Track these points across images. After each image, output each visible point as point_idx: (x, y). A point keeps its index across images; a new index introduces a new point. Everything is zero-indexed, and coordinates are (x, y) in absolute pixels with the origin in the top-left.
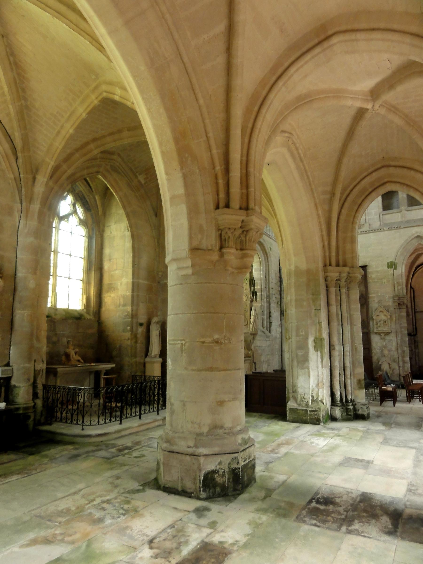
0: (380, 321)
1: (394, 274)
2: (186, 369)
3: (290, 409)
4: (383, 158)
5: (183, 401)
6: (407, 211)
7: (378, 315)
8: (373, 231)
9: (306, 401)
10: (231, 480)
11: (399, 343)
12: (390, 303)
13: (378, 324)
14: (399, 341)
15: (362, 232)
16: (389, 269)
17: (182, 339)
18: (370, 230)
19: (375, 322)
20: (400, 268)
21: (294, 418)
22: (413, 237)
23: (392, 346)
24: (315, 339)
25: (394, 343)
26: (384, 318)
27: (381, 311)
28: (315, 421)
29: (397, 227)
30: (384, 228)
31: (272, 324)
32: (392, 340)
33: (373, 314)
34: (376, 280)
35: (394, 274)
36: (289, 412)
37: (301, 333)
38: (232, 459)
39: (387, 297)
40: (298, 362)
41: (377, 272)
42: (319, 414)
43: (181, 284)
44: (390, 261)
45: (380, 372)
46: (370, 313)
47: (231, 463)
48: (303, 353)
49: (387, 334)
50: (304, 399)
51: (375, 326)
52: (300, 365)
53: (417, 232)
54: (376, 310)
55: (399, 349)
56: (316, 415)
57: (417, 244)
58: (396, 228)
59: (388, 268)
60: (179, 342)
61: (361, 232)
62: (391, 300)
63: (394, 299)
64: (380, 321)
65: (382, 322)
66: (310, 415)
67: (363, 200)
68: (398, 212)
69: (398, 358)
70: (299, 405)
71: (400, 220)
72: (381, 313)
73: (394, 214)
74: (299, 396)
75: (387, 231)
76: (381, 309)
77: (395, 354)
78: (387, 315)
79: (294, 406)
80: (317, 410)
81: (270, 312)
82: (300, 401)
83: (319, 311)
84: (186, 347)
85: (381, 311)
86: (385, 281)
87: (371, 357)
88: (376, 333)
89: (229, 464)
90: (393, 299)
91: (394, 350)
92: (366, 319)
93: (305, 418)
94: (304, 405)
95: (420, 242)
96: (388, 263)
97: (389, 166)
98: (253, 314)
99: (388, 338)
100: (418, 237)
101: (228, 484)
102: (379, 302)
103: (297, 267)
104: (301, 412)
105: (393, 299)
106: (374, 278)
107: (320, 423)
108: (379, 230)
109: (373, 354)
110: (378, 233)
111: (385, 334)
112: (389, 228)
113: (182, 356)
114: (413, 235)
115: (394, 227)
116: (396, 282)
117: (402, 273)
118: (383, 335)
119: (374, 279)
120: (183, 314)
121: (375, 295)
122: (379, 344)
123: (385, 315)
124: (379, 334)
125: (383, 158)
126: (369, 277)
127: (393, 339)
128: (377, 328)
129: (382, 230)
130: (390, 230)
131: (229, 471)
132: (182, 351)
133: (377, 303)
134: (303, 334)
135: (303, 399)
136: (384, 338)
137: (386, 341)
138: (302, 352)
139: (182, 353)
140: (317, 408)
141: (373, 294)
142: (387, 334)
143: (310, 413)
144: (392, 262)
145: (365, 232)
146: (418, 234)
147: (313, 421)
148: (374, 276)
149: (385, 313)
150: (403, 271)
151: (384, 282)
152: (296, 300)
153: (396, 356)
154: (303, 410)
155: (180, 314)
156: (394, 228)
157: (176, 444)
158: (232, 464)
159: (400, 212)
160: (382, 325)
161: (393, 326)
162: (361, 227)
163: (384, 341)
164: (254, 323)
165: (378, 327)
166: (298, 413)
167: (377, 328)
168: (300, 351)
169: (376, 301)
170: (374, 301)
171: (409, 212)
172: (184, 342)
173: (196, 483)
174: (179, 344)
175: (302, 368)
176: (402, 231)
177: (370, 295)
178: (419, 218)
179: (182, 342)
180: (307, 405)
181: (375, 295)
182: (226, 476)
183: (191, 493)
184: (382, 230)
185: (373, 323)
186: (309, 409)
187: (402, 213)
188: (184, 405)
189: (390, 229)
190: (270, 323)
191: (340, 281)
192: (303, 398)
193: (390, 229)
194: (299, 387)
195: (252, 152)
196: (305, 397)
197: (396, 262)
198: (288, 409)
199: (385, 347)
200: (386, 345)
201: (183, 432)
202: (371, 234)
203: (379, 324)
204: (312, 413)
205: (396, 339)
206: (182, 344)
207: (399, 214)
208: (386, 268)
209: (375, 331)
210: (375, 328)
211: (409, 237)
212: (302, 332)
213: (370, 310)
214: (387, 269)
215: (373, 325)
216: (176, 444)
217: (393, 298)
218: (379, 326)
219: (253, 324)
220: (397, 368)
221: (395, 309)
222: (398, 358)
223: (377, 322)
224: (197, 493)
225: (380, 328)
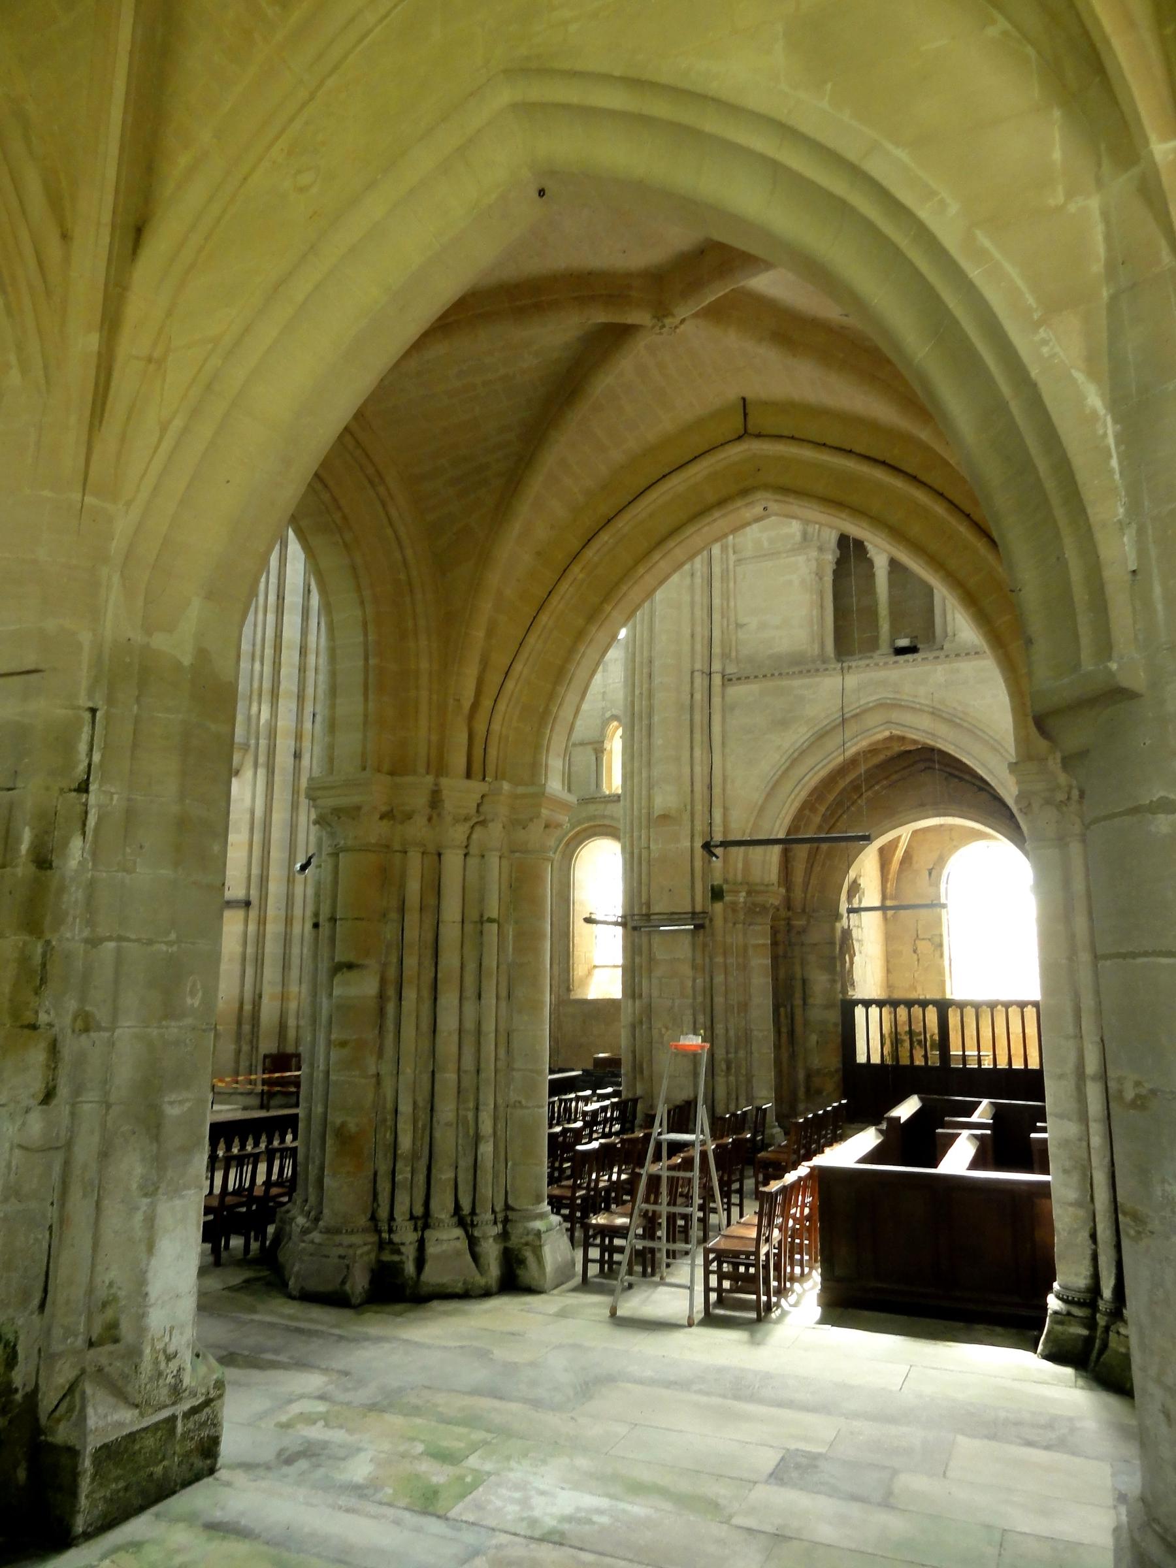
3: (110, 1453)
21: (109, 1501)
28: (199, 1463)
36: (93, 1479)
37: (189, 1001)
42: (216, 1416)
48: (187, 1105)
52: (170, 1173)
56: (205, 1423)
79: (120, 1425)
82: (151, 1379)
94: (163, 1394)
104: (150, 1442)
107: (215, 1464)
138: (181, 1102)
143: (184, 1425)
147: (192, 1465)
168: (174, 1097)
192: (162, 1358)
194: (153, 1295)
196: (171, 1350)
212: (193, 994)
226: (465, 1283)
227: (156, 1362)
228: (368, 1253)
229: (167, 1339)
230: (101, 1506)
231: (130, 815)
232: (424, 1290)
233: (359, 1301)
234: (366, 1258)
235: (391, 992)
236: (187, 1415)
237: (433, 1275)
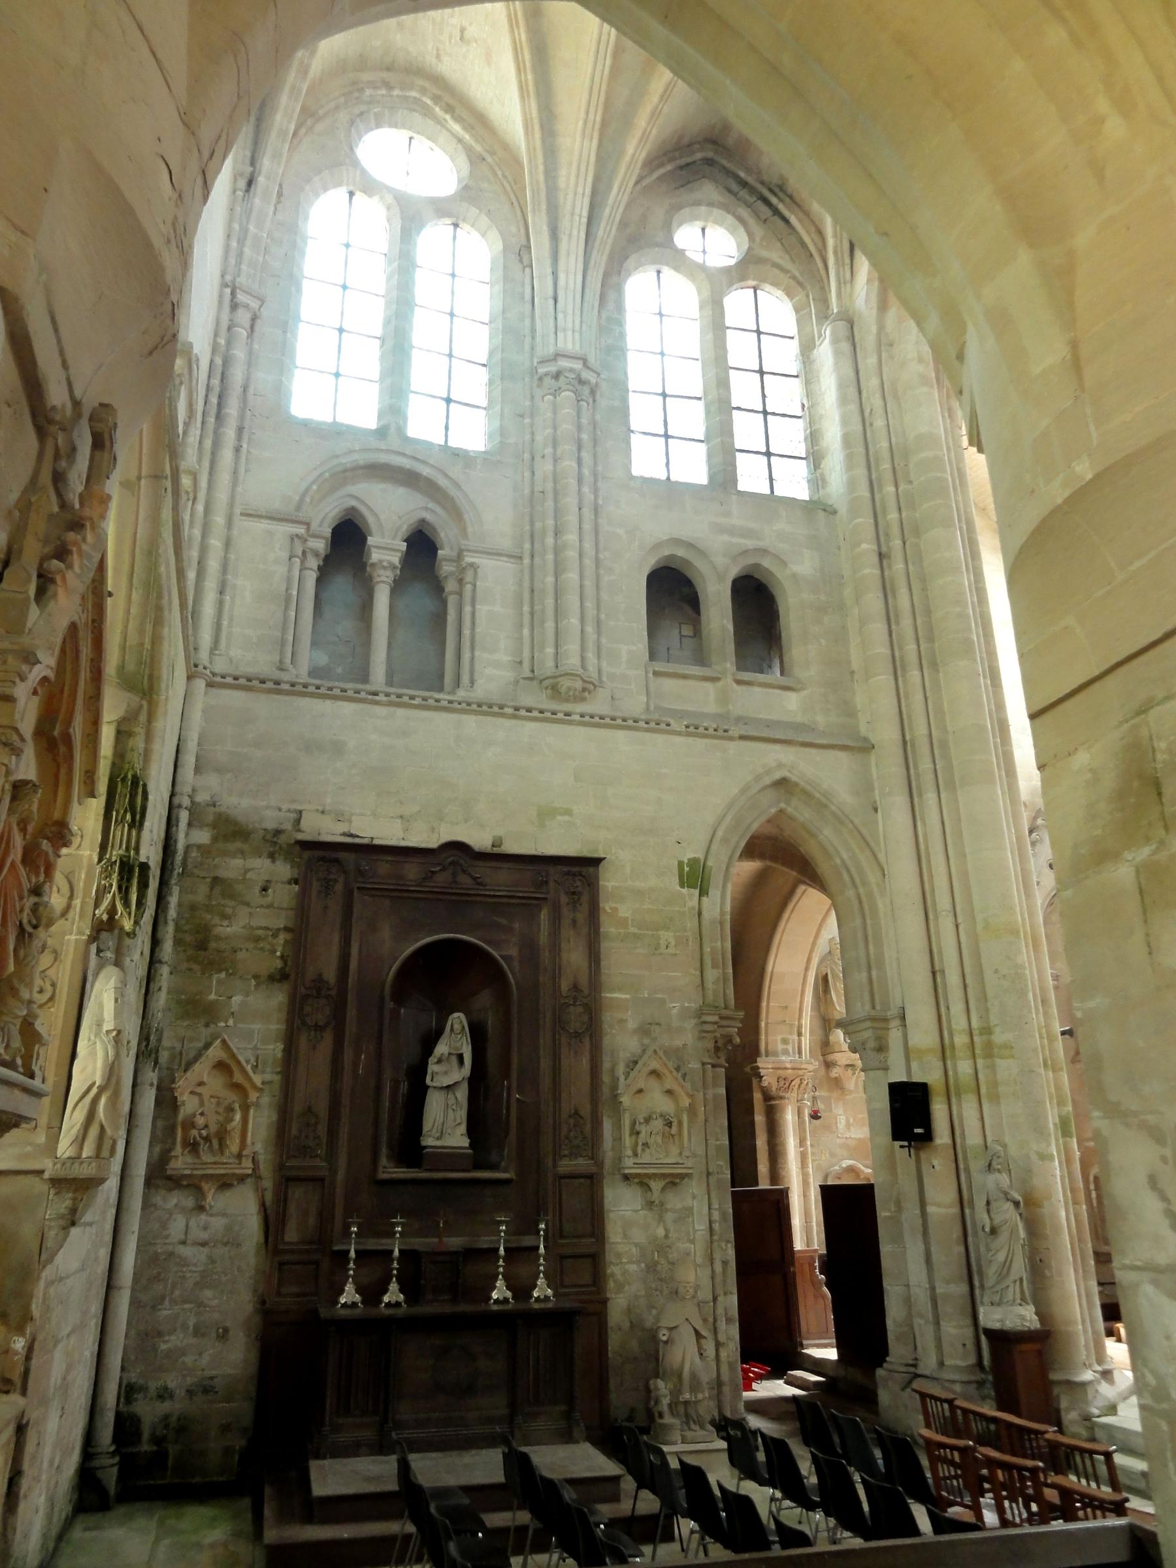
0: (647, 1120)
1: (705, 914)
7: (640, 1091)
11: (716, 1226)
12: (686, 1037)
13: (638, 1133)
14: (716, 1215)
15: (587, 719)
16: (685, 891)
18: (618, 714)
20: (719, 893)
23: (692, 1242)
25: (701, 1227)
27: (654, 1073)
30: (672, 722)
32: (690, 1209)
34: (633, 930)
35: (700, 914)
39: (675, 1011)
41: (639, 894)
44: (691, 855)
46: (606, 1078)
49: (674, 1181)
51: (628, 1141)
53: (780, 766)
57: (773, 811)
59: (682, 886)
61: (582, 716)
62: (690, 1024)
63: (705, 1022)
64: (647, 1120)
65: (658, 1124)
69: (715, 1299)
71: (712, 708)
72: (653, 1083)
75: (679, 734)
76: (654, 1065)
77: (705, 1275)
85: (654, 1073)
86: (666, 936)
87: (604, 1302)
88: (626, 1178)
90: (695, 1021)
91: (699, 1260)
92: (588, 1107)
95: (783, 805)
96: (681, 864)
98: (109, 1025)
99: (675, 1201)
102: (644, 1030)
105: (695, 1021)
106: (626, 919)
108: (653, 725)
109: (611, 1284)
110: (647, 735)
111: (668, 1180)
112: (687, 727)
114: (768, 772)
116: (707, 950)
117: (722, 913)
118: (656, 1186)
119: (623, 922)
121: (628, 996)
122: (638, 1236)
123: (669, 1092)
124: (642, 1182)
126: (605, 911)
127: (695, 1209)
128: (636, 1155)
129: (663, 726)
130: (689, 735)
133: (635, 1031)
136: (662, 1204)
137: (669, 1217)
141: (620, 990)
142: (674, 1181)
144: (693, 862)
145: (597, 719)
148: (625, 911)
149: (669, 1083)
150: (728, 908)
151: (663, 943)
156: (706, 729)
162: (586, 694)
163: (661, 1219)
164: (102, 1089)
165: (639, 1148)
167: (636, 1155)
169: (632, 1025)
170: (622, 1021)
171: (744, 688)
176: (733, 747)
177: (608, 995)
178: (774, 717)
181: (628, 996)
184: (663, 726)
185: (618, 1126)
187: (720, 684)
189: (692, 729)
197: (710, 863)
199: (662, 1248)
200: (666, 1236)
202: (621, 735)
203: (644, 1129)
207: (708, 685)
208: (672, 882)
209: (629, 1165)
210: (629, 1152)
214: (678, 888)
215: (618, 1139)
217: (700, 1018)
218: (646, 1145)
219: (95, 1102)
221: (703, 1064)
222: (715, 1299)
223: (634, 1123)
225: (648, 1151)
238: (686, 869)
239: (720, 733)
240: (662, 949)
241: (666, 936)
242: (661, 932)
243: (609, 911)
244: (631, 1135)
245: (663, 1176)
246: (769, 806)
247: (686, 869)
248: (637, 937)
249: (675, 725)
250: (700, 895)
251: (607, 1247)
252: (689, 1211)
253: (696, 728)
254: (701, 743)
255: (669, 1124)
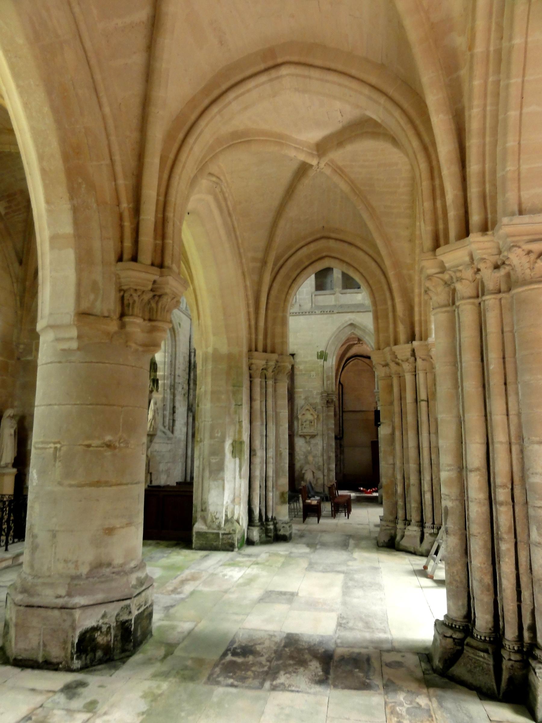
0: (305, 421)
1: (325, 366)
2: (60, 484)
4: (323, 227)
5: (53, 531)
6: (342, 294)
7: (304, 414)
8: (303, 313)
9: (218, 521)
10: (119, 638)
11: (325, 448)
12: (318, 400)
13: (303, 425)
14: (325, 445)
16: (319, 360)
17: (57, 440)
19: (300, 422)
22: (346, 325)
24: (234, 443)
25: (320, 448)
26: (309, 417)
27: (307, 410)
28: (228, 547)
29: (330, 311)
30: (316, 311)
31: (176, 422)
33: (299, 412)
34: (304, 372)
35: (323, 366)
37: (216, 435)
38: (122, 608)
39: (315, 393)
40: (211, 472)
41: (306, 362)
43: (60, 362)
44: (321, 350)
45: (302, 483)
46: (295, 411)
47: (121, 614)
48: (217, 460)
50: (216, 519)
53: (350, 320)
54: (302, 408)
55: (325, 455)
56: (230, 538)
57: (349, 333)
58: (328, 312)
59: (318, 358)
60: (52, 445)
62: (319, 396)
63: (322, 396)
64: (305, 421)
65: (308, 422)
66: (223, 539)
67: (298, 275)
68: (331, 294)
69: (324, 465)
70: (209, 527)
71: (333, 303)
72: (308, 412)
73: (327, 296)
74: (210, 515)
75: (319, 314)
76: (307, 407)
77: (321, 460)
78: (314, 414)
79: (201, 529)
80: (231, 532)
81: (174, 407)
82: (211, 522)
83: (241, 406)
84: (62, 452)
89: (118, 615)
91: (319, 455)
93: (215, 544)
94: (215, 526)
95: (353, 331)
96: (318, 353)
97: (329, 238)
98: (153, 409)
99: (313, 441)
100: (351, 324)
101: (114, 644)
102: (306, 399)
103: (215, 350)
104: (211, 536)
109: (296, 461)
113: (54, 465)
114: (346, 322)
115: (326, 310)
116: (325, 376)
117: (332, 365)
118: (308, 438)
119: (301, 371)
120: (59, 405)
122: (304, 450)
123: (312, 414)
124: (304, 436)
125: (323, 227)
128: (302, 430)
131: (117, 626)
132: (55, 458)
133: (303, 399)
134: (219, 435)
135: (214, 520)
136: (309, 442)
137: (312, 445)
138: (216, 459)
139: (55, 461)
140: (231, 530)
142: (313, 436)
143: (222, 536)
144: (322, 352)
146: (352, 322)
148: (302, 367)
149: (311, 412)
150: (334, 363)
151: (312, 375)
152: (213, 393)
153: (321, 463)
154: (213, 533)
155: (56, 404)
156: (327, 312)
157: (38, 595)
158: (122, 616)
159: (334, 294)
160: (308, 426)
161: (320, 427)
163: (309, 445)
164: (153, 420)
165: (303, 429)
166: (207, 537)
167: (302, 430)
168: (213, 457)
169: (303, 397)
170: (300, 397)
171: (344, 295)
172: (58, 446)
173: (67, 649)
174: (51, 448)
175: (215, 480)
176: (335, 316)
178: (353, 303)
179: (56, 445)
180: (219, 527)
182: (111, 634)
183: (58, 664)
184: (313, 313)
186: (221, 532)
187: (336, 295)
188: (54, 536)
189: (322, 312)
190: (174, 421)
191: (267, 371)
193: (323, 313)
195: (173, 192)
196: (217, 516)
198: (194, 533)
199: (310, 452)
200: (311, 449)
201: (49, 576)
203: (304, 424)
204: (225, 536)
205: (322, 443)
206: (56, 448)
207: (333, 297)
208: (315, 358)
209: (300, 433)
211: (343, 324)
212: (218, 432)
213: (295, 408)
214: (317, 359)
215: (298, 426)
216: (38, 595)
218: (305, 427)
219: (152, 421)
220: (322, 477)
221: (323, 407)
222: (324, 465)
223: (302, 422)
224: (67, 662)
226: (414, 548)
227: (212, 518)
228: (389, 530)
229: (215, 514)
230: (199, 545)
231: (206, 391)
232: (401, 547)
233: (381, 545)
234: (389, 532)
235: (397, 434)
236: (223, 534)
237: (405, 543)
238: (319, 354)
239: (331, 312)
240: (312, 377)
241: (313, 373)
242: (311, 372)
243: (297, 368)
244: (301, 425)
245: (310, 435)
246: (348, 332)
247: (319, 354)
248: (304, 374)
249: (317, 312)
250: (324, 360)
251: (295, 452)
252: (317, 444)
253: (324, 312)
254: (326, 316)
255: (312, 422)
